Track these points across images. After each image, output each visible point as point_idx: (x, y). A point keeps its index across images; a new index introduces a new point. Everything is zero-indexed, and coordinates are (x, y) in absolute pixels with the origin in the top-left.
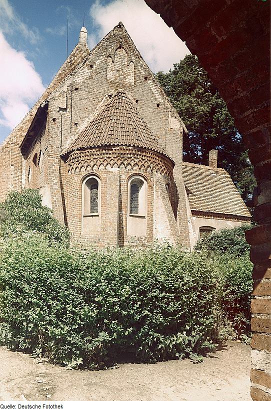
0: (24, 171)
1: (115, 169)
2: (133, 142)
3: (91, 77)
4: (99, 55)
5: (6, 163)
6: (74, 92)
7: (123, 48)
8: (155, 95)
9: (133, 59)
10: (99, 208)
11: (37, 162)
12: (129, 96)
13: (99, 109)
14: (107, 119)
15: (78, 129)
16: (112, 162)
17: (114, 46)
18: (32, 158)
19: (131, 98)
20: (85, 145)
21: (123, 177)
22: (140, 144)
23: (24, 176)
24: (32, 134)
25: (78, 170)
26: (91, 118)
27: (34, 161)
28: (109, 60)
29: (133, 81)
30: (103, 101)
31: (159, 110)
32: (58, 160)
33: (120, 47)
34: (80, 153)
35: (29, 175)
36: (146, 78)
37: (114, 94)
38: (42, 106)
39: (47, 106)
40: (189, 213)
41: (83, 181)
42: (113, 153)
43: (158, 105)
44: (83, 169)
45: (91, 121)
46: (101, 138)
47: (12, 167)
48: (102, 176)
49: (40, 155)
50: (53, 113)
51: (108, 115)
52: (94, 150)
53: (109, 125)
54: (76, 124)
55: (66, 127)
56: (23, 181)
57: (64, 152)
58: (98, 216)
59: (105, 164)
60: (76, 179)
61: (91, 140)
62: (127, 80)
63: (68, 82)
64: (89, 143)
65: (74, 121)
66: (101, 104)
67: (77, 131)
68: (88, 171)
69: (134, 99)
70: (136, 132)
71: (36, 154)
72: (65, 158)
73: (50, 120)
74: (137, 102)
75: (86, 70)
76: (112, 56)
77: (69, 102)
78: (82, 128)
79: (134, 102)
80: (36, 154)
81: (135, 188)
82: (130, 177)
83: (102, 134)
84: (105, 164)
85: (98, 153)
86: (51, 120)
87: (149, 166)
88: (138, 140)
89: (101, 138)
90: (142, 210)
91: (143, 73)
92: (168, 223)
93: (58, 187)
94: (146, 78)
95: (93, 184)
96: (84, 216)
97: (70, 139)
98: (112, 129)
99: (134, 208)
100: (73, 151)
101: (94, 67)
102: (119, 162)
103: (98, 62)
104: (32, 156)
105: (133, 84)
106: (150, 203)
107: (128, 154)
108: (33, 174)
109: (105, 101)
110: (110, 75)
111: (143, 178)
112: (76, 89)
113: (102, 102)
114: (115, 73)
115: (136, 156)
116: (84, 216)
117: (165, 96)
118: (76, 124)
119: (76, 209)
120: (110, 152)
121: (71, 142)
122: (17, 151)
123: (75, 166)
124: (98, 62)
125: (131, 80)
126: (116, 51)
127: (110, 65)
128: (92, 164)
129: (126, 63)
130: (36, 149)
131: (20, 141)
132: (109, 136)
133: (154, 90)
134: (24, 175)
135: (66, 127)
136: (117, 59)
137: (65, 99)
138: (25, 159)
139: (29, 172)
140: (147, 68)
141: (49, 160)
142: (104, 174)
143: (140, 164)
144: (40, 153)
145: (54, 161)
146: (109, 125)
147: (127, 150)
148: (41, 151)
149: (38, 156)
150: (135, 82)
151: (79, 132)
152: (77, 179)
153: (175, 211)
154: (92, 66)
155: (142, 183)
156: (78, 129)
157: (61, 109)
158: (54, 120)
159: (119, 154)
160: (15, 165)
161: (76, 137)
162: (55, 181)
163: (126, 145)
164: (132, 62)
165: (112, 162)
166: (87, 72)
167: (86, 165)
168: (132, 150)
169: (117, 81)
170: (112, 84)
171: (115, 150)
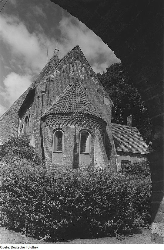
0: (19, 126)
1: (73, 126)
2: (83, 111)
3: (60, 75)
4: (65, 63)
6: (50, 82)
7: (79, 59)
9: (84, 65)
10: (63, 148)
12: (81, 86)
13: (64, 93)
14: (69, 98)
16: (71, 122)
18: (24, 118)
19: (82, 87)
20: (55, 112)
21: (77, 130)
22: (87, 112)
23: (19, 129)
25: (51, 126)
26: (60, 97)
27: (26, 120)
28: (71, 65)
29: (84, 77)
30: (66, 88)
31: (98, 94)
33: (77, 59)
34: (52, 117)
35: (22, 128)
36: (91, 76)
37: (73, 84)
39: (34, 90)
40: (115, 152)
41: (54, 132)
42: (71, 117)
43: (98, 91)
44: (54, 126)
45: (59, 99)
46: (65, 109)
47: (13, 124)
49: (29, 117)
50: (38, 93)
51: (69, 96)
53: (69, 102)
54: (51, 100)
55: (45, 102)
56: (19, 132)
58: (62, 152)
59: (67, 123)
60: (50, 131)
61: (59, 110)
62: (81, 77)
63: (47, 77)
64: (58, 111)
65: (50, 98)
69: (84, 87)
70: (85, 106)
71: (27, 116)
72: (44, 119)
73: (36, 98)
74: (86, 89)
75: (57, 71)
76: (72, 63)
77: (47, 88)
78: (54, 102)
80: (27, 116)
83: (66, 106)
85: (63, 116)
87: (92, 125)
88: (86, 110)
89: (65, 109)
90: (87, 150)
91: (90, 73)
92: (103, 158)
93: (39, 135)
95: (59, 135)
96: (54, 153)
98: (71, 103)
99: (83, 149)
100: (49, 115)
101: (62, 69)
103: (64, 67)
104: (24, 117)
105: (84, 79)
106: (93, 146)
107: (80, 118)
108: (25, 128)
110: (71, 73)
111: (89, 131)
112: (52, 81)
113: (66, 89)
114: (74, 73)
115: (84, 119)
116: (54, 153)
117: (102, 86)
120: (70, 116)
121: (47, 110)
122: (16, 115)
123: (49, 124)
124: (64, 67)
125: (82, 76)
126: (75, 60)
127: (71, 68)
128: (59, 123)
129: (80, 67)
130: (27, 114)
131: (18, 109)
132: (69, 107)
133: (95, 82)
134: (20, 128)
135: (45, 102)
136: (75, 65)
137: (45, 86)
138: (21, 119)
139: (22, 127)
143: (87, 124)
144: (30, 116)
145: (37, 120)
146: (69, 102)
147: (80, 115)
148: (30, 114)
149: (28, 117)
150: (85, 78)
151: (53, 105)
152: (50, 131)
153: (109, 159)
154: (61, 69)
157: (42, 92)
158: (38, 97)
159: (75, 117)
160: (14, 122)
161: (51, 107)
162: (38, 132)
163: (79, 113)
164: (84, 67)
165: (71, 122)
166: (58, 72)
167: (56, 123)
168: (83, 116)
169: (75, 77)
170: (72, 78)
171: (73, 115)
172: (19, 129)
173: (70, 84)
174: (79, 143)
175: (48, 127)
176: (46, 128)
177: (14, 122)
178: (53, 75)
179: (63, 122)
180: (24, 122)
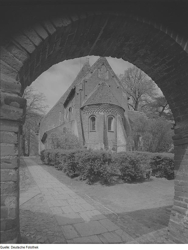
1: (102, 113)
2: (109, 103)
3: (92, 77)
4: (95, 68)
6: (86, 83)
10: (96, 128)
11: (71, 110)
16: (101, 110)
17: (101, 64)
18: (68, 109)
20: (90, 104)
21: (105, 116)
24: (68, 99)
25: (87, 114)
27: (69, 110)
36: (113, 77)
37: (101, 83)
38: (73, 88)
43: (118, 88)
50: (77, 91)
54: (86, 96)
55: (83, 97)
57: (82, 106)
59: (98, 111)
72: (82, 109)
73: (76, 94)
78: (88, 97)
79: (109, 87)
80: (70, 107)
81: (110, 120)
82: (108, 116)
84: (98, 111)
85: (94, 107)
86: (77, 94)
87: (115, 112)
90: (112, 129)
93: (79, 120)
94: (113, 77)
95: (93, 119)
98: (100, 97)
99: (109, 128)
102: (104, 110)
103: (94, 71)
104: (68, 108)
108: (69, 115)
109: (97, 86)
110: (99, 75)
112: (86, 82)
115: (110, 108)
118: (86, 96)
122: (62, 106)
123: (86, 112)
124: (94, 71)
125: (107, 78)
127: (99, 72)
128: (93, 111)
130: (70, 105)
131: (64, 102)
135: (83, 97)
136: (102, 69)
137: (82, 86)
140: (113, 73)
141: (75, 111)
143: (112, 111)
150: (109, 79)
152: (87, 117)
154: (92, 73)
155: (112, 118)
158: (78, 94)
161: (86, 100)
162: (79, 118)
165: (101, 110)
166: (90, 75)
167: (91, 111)
172: (65, 116)
174: (107, 125)
175: (85, 114)
176: (84, 115)
178: (87, 78)
179: (96, 111)
180: (68, 111)
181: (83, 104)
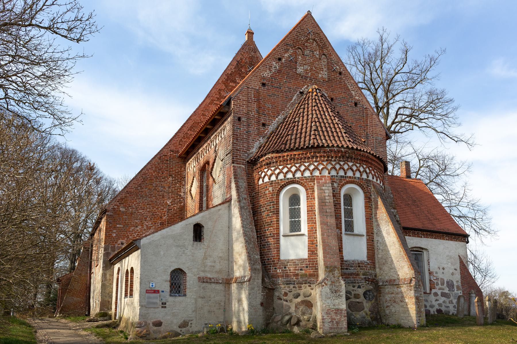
5: (163, 173)
8: (352, 92)
15: (267, 131)
30: (294, 98)
32: (244, 166)
42: (321, 156)
47: (171, 179)
48: (308, 184)
52: (295, 153)
66: (292, 102)
67: (265, 132)
68: (288, 179)
69: (328, 96)
97: (258, 141)
119: (272, 227)
120: (318, 155)
121: (259, 146)
142: (309, 182)
145: (240, 167)
156: (267, 131)
173: (301, 91)
176: (261, 182)
177: (174, 176)
181: (254, 150)
